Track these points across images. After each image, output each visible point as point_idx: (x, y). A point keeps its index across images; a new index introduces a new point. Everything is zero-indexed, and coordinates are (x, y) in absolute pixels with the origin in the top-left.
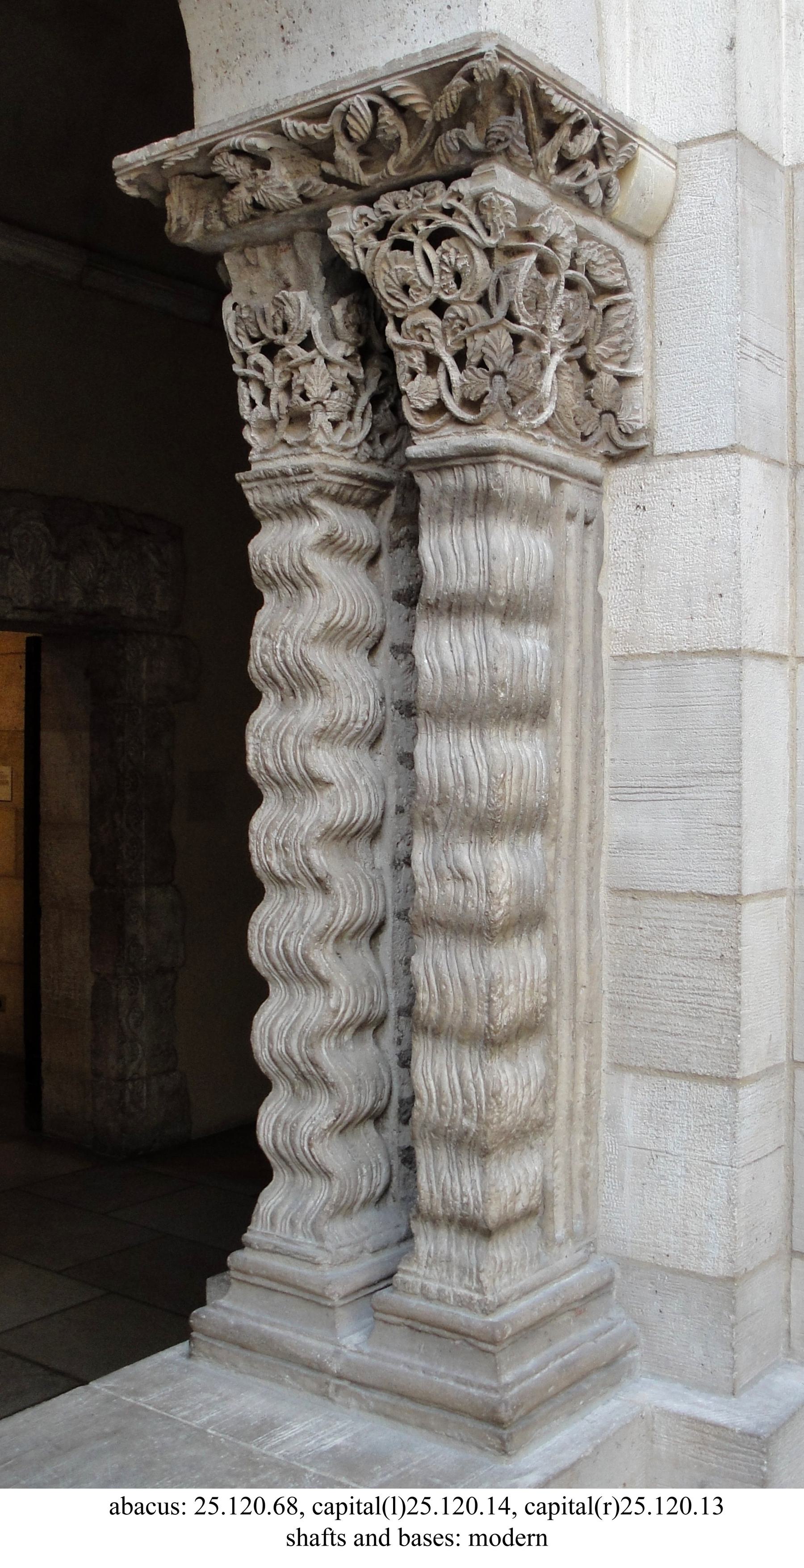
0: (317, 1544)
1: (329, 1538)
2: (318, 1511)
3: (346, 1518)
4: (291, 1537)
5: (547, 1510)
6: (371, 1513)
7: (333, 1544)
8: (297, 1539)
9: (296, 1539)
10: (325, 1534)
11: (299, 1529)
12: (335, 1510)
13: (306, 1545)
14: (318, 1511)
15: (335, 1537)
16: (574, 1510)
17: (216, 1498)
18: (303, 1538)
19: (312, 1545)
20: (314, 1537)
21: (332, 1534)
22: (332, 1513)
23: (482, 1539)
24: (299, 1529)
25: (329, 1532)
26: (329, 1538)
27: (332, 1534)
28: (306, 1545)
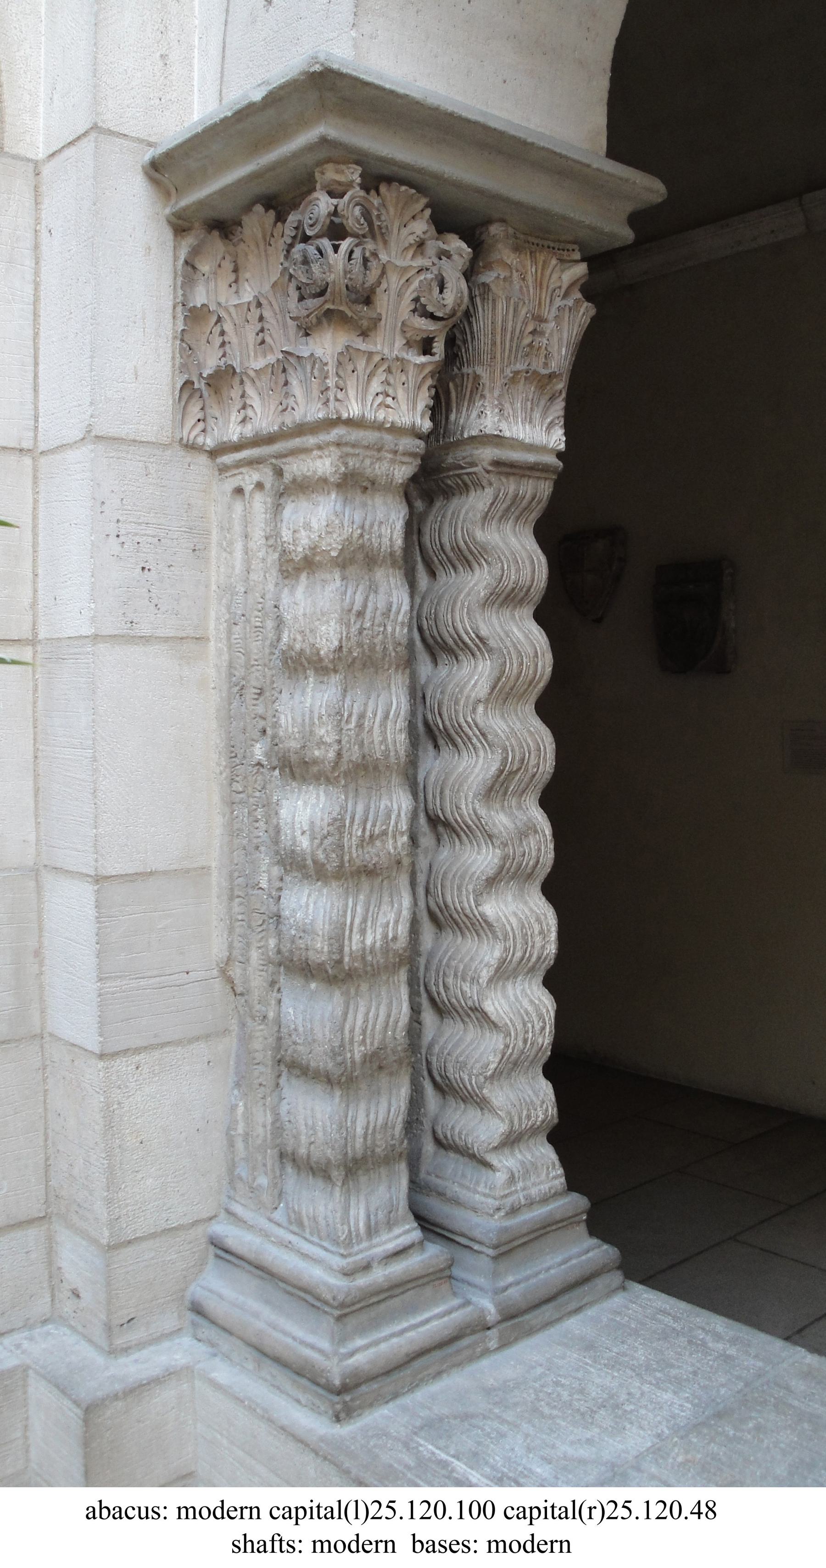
0: (265, 1551)
1: (277, 1544)
2: (509, 1516)
3: (305, 1523)
4: (236, 1543)
5: (293, 1514)
6: (332, 1518)
7: (281, 1551)
8: (242, 1546)
9: (242, 1546)
10: (273, 1541)
11: (245, 1535)
12: (294, 1514)
13: (253, 1551)
14: (275, 1515)
15: (284, 1544)
16: (556, 1515)
17: (630, 1502)
18: (249, 1545)
19: (259, 1551)
20: (262, 1543)
21: (281, 1541)
22: (525, 1518)
23: (326, 1545)
24: (245, 1535)
25: (277, 1538)
26: (277, 1544)
27: (281, 1541)
28: (253, 1551)
